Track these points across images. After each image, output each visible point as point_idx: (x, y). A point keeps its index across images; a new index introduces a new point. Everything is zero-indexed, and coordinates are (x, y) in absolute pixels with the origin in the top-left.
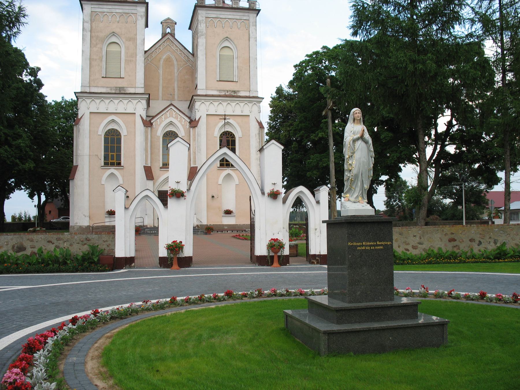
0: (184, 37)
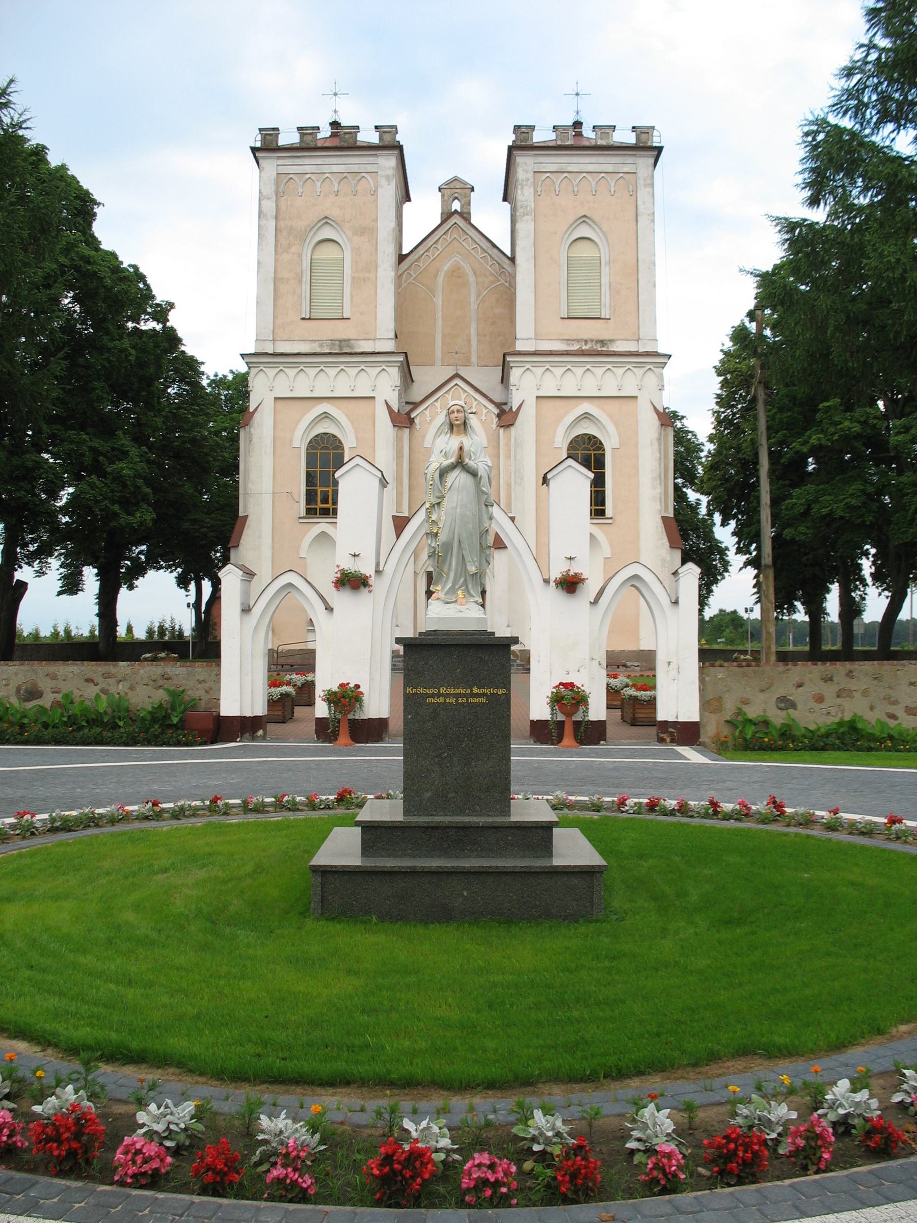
0: (491, 218)
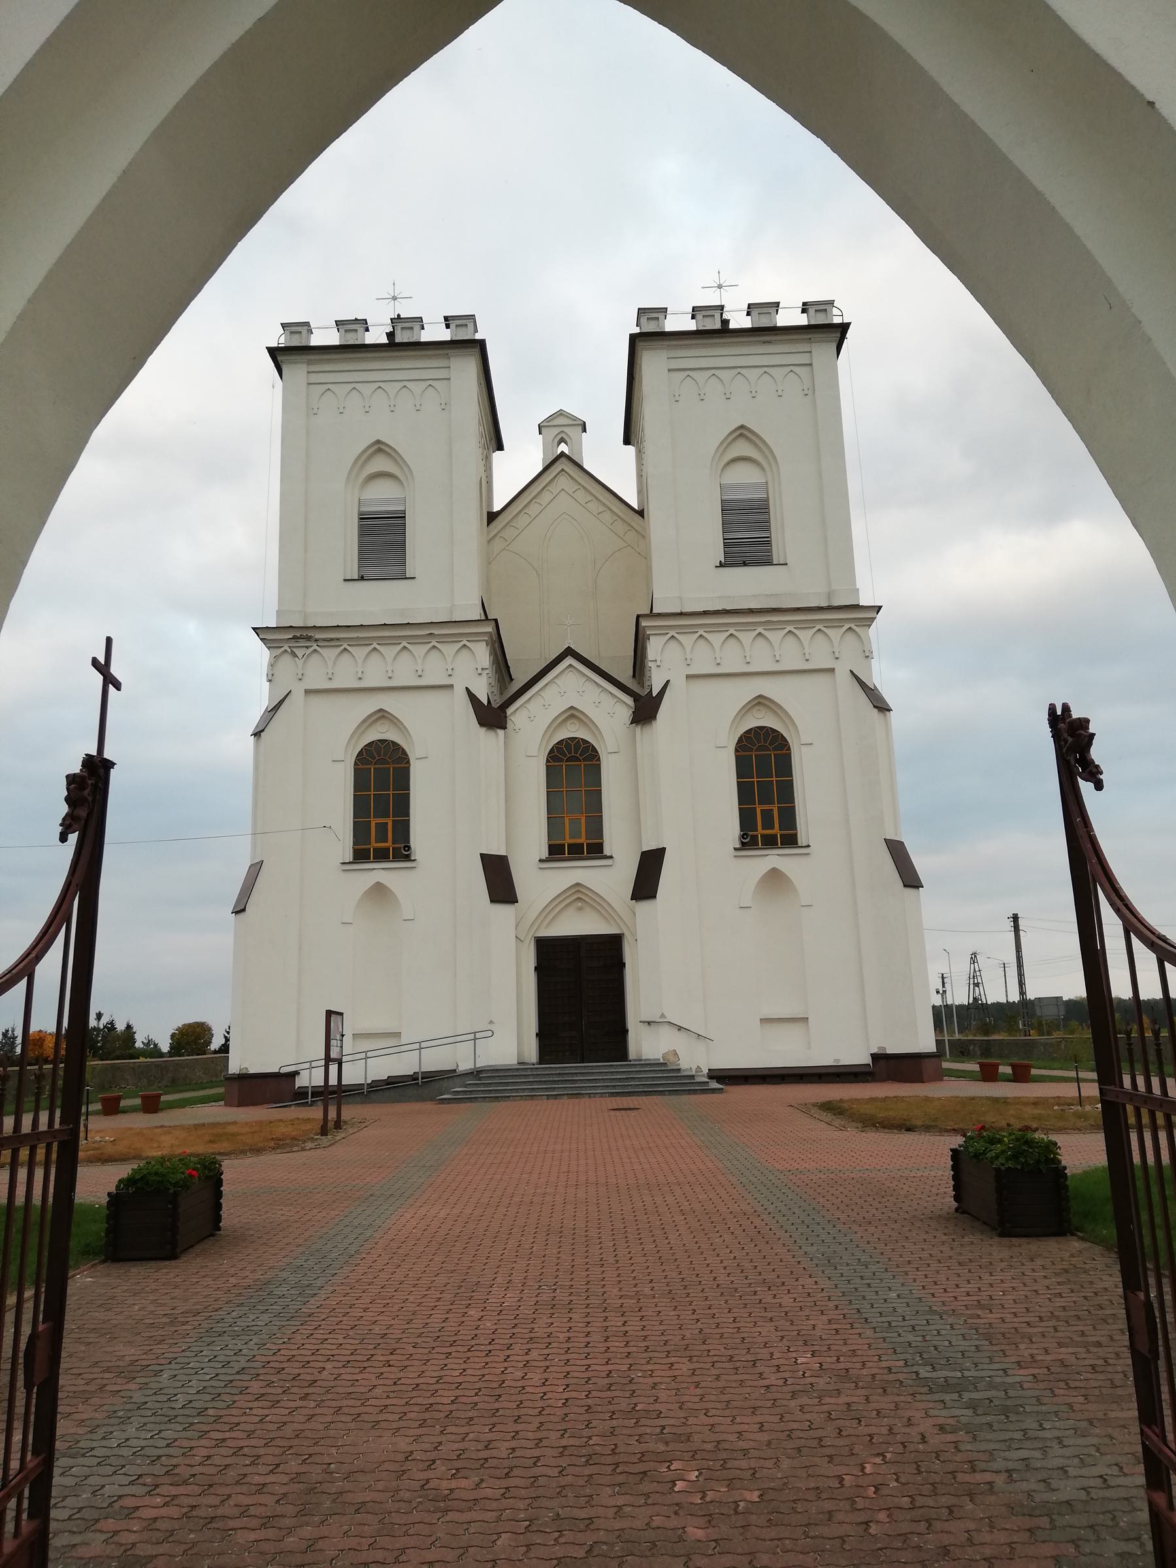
0: (611, 463)
